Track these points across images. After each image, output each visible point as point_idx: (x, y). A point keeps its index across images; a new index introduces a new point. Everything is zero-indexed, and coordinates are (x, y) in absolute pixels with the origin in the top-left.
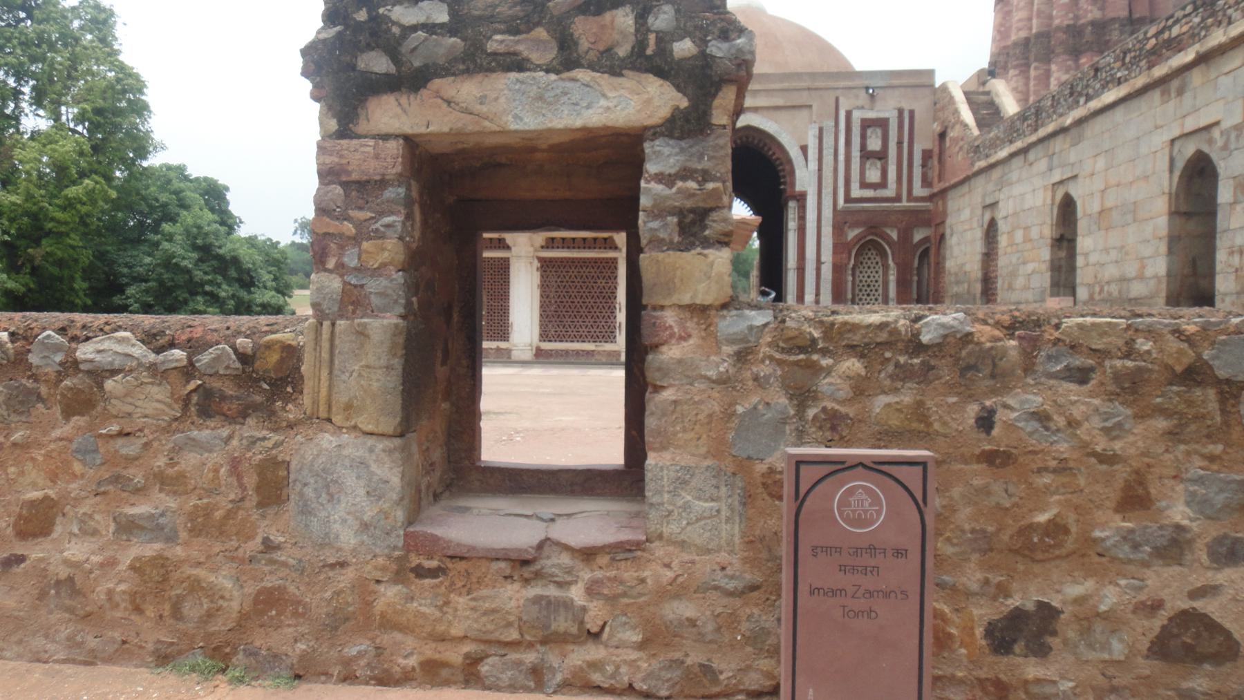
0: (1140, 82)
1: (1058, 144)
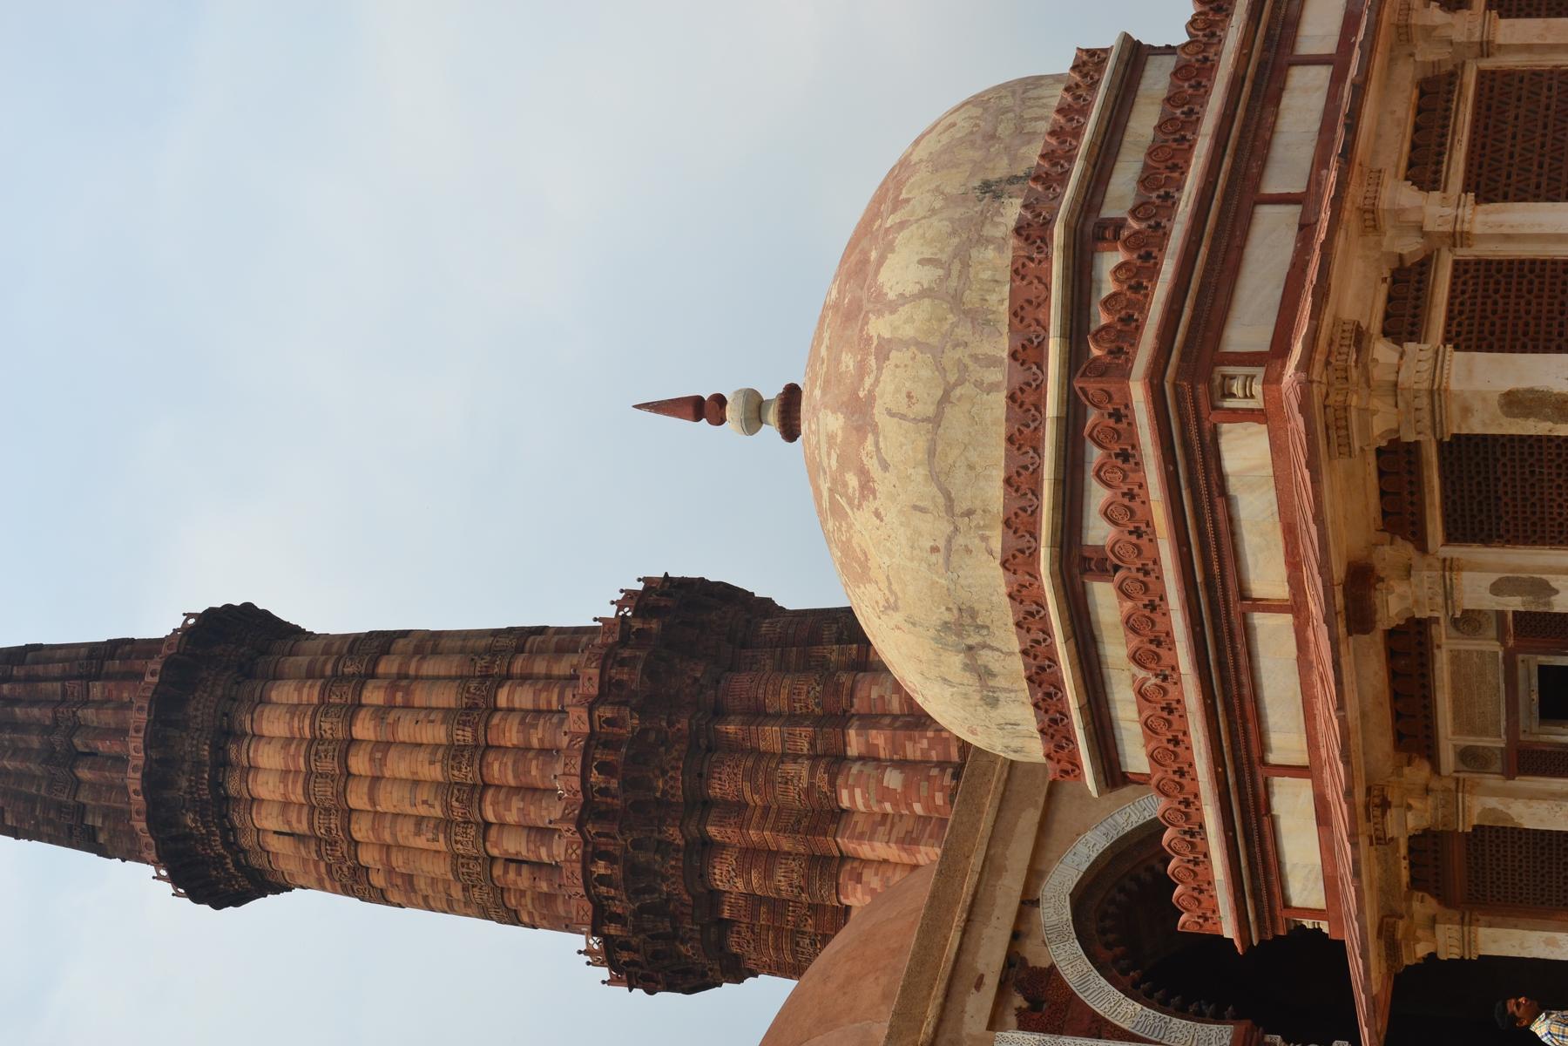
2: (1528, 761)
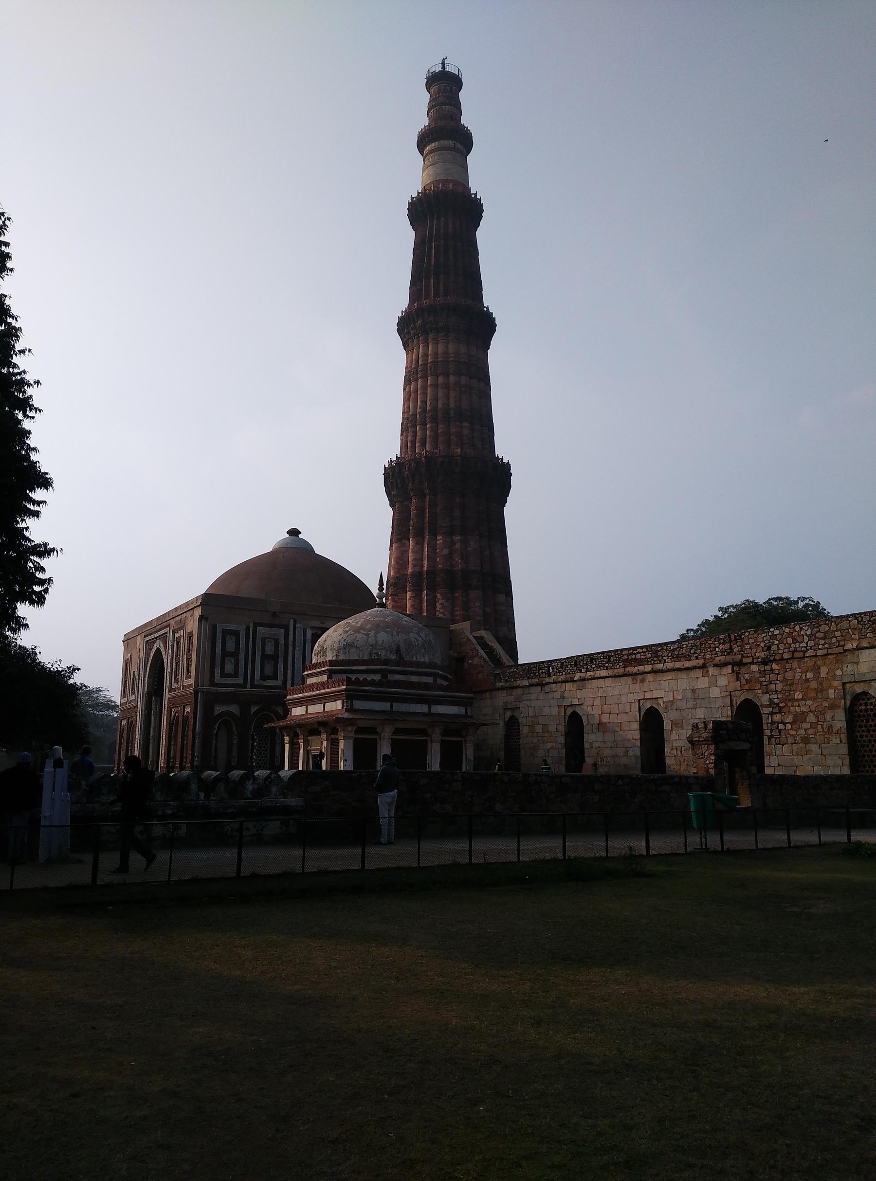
0: (621, 671)
1: (569, 686)
2: (307, 753)
